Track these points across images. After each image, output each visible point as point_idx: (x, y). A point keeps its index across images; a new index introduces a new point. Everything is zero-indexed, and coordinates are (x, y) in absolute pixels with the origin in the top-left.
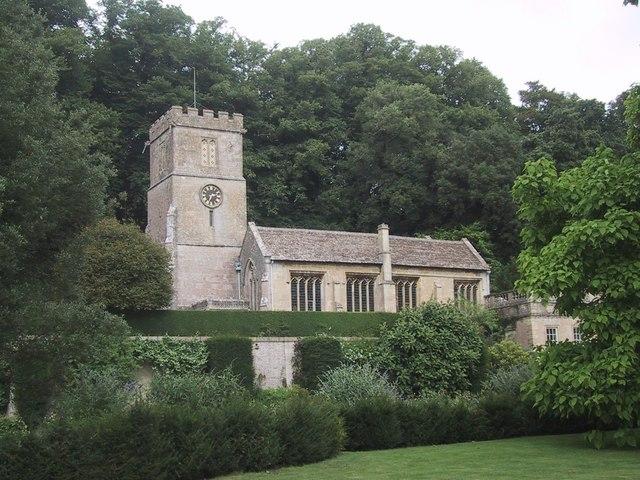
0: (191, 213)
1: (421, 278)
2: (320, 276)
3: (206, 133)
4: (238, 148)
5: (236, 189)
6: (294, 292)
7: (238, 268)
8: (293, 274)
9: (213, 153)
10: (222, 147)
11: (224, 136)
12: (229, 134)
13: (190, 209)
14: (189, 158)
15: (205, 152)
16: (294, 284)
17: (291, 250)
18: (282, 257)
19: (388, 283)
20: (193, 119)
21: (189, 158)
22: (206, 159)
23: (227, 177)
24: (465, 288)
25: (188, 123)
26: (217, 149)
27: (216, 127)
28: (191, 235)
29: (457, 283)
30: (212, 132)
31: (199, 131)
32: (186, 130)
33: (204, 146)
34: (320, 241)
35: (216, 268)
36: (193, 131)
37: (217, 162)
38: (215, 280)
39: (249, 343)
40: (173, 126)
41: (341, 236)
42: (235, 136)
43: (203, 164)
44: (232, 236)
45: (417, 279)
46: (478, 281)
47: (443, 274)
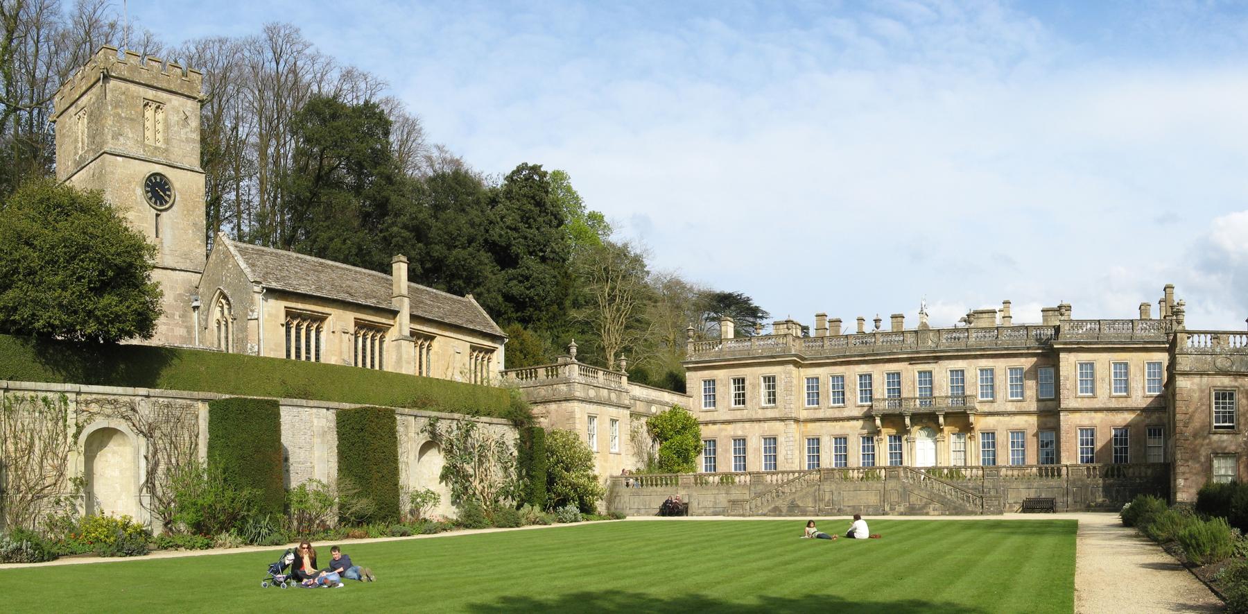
3: (150, 94)
4: (194, 123)
7: (195, 304)
9: (160, 127)
11: (176, 101)
12: (181, 99)
20: (133, 69)
23: (179, 165)
25: (126, 74)
26: (166, 120)
27: (165, 85)
30: (160, 93)
31: (142, 91)
32: (122, 85)
33: (149, 113)
36: (132, 87)
39: (276, 405)
40: (106, 77)
42: (190, 102)
44: (186, 256)
46: (492, 351)
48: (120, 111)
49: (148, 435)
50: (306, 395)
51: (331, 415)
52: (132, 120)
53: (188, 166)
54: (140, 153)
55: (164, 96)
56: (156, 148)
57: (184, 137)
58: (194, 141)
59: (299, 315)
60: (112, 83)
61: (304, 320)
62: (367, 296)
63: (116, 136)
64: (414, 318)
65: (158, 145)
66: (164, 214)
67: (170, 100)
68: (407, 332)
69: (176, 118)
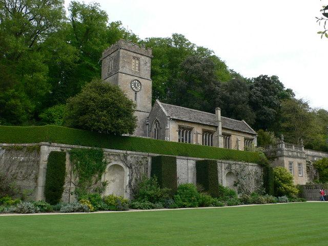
4: (149, 65)
8: (180, 127)
9: (137, 65)
10: (142, 63)
11: (143, 58)
14: (127, 65)
15: (134, 64)
20: (129, 47)
21: (127, 65)
22: (134, 67)
24: (248, 141)
26: (139, 64)
27: (140, 52)
37: (139, 70)
39: (175, 158)
40: (120, 48)
42: (148, 58)
44: (144, 107)
47: (240, 134)
49: (130, 167)
50: (186, 155)
51: (194, 162)
53: (146, 78)
54: (131, 73)
55: (139, 56)
59: (183, 128)
60: (121, 51)
61: (185, 129)
62: (206, 121)
63: (123, 67)
64: (223, 128)
68: (220, 133)
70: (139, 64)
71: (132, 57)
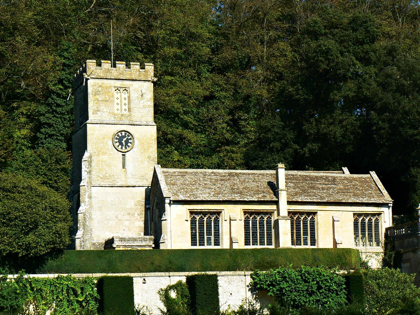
0: (105, 158)
1: (319, 212)
2: (218, 213)
3: (118, 83)
5: (146, 134)
6: (193, 228)
9: (126, 102)
10: (134, 95)
13: (104, 153)
14: (102, 107)
16: (193, 222)
17: (192, 191)
18: (181, 197)
19: (284, 218)
23: (137, 123)
25: (102, 75)
26: (129, 97)
27: (128, 77)
28: (104, 178)
29: (357, 215)
31: (112, 81)
34: (222, 180)
35: (128, 207)
37: (129, 110)
38: (127, 217)
41: (244, 174)
43: (116, 112)
45: (315, 213)
48: (98, 97)
52: (106, 101)
56: (122, 115)
57: (141, 106)
58: (149, 106)
65: (124, 112)
66: (127, 154)
67: (132, 85)
69: (136, 95)
70: (129, 97)
71: (114, 89)
